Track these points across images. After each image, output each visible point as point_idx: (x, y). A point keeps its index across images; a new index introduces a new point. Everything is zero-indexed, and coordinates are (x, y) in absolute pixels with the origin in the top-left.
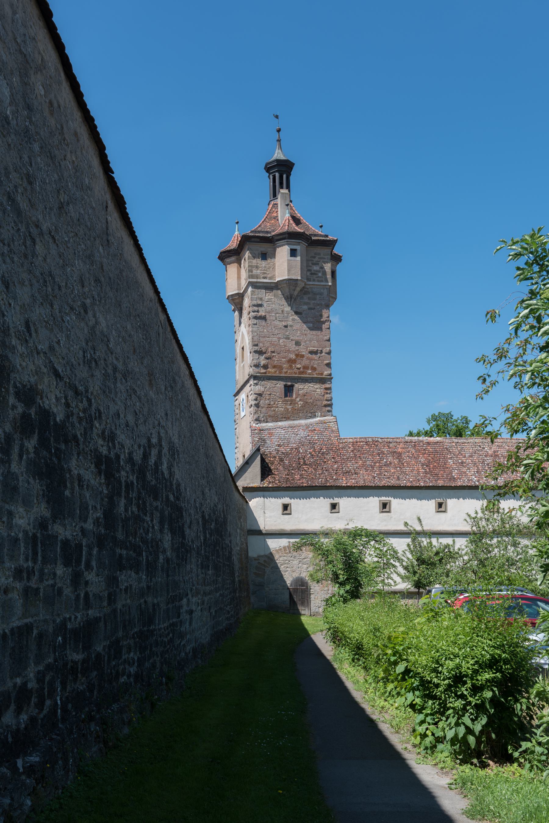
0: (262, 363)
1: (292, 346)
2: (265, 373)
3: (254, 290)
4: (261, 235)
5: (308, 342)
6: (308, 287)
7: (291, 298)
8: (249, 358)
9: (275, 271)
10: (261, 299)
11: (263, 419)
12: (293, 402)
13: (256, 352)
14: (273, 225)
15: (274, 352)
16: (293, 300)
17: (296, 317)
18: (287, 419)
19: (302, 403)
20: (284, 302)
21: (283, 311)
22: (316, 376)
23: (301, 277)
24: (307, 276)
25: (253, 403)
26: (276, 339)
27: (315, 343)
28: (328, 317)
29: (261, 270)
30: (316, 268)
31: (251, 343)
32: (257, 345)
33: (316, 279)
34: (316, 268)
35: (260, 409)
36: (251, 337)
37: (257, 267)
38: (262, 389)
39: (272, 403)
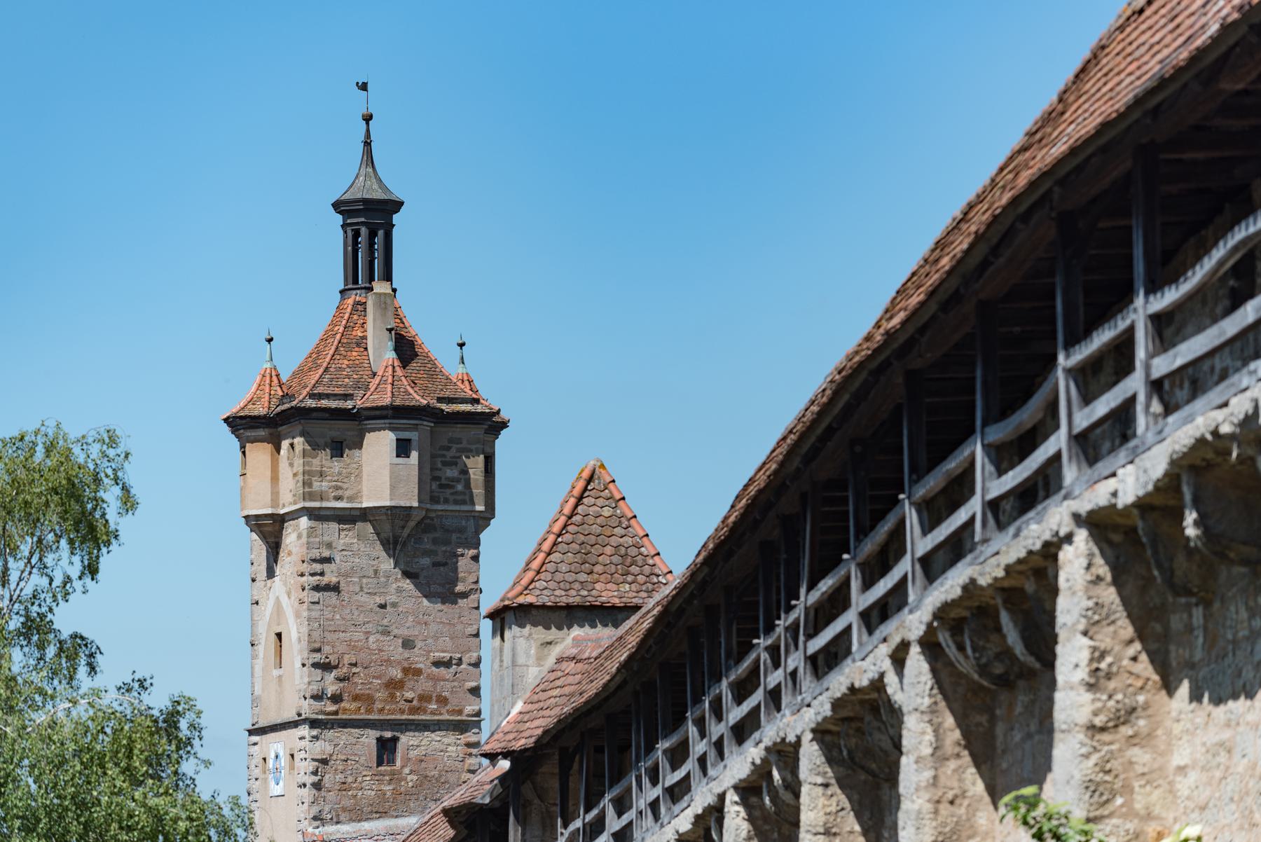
0: (331, 689)
1: (398, 653)
2: (336, 713)
3: (313, 523)
4: (333, 404)
5: (430, 641)
6: (433, 515)
7: (396, 543)
8: (297, 676)
9: (360, 483)
10: (329, 546)
11: (329, 816)
12: (395, 778)
13: (316, 665)
14: (354, 367)
15: (355, 665)
16: (399, 547)
17: (407, 584)
18: (383, 814)
19: (415, 778)
20: (379, 551)
21: (376, 572)
22: (446, 717)
23: (420, 501)
24: (432, 491)
25: (310, 779)
26: (362, 637)
27: (446, 642)
28: (477, 582)
29: (331, 481)
30: (451, 473)
31: (305, 644)
32: (318, 650)
33: (451, 498)
34: (451, 473)
35: (323, 793)
36: (305, 630)
37: (321, 474)
38: (329, 749)
39: (350, 779)
